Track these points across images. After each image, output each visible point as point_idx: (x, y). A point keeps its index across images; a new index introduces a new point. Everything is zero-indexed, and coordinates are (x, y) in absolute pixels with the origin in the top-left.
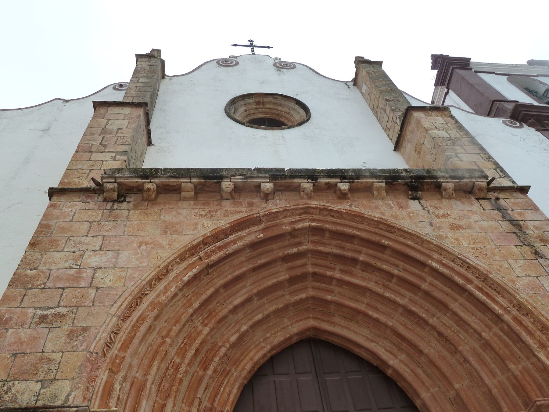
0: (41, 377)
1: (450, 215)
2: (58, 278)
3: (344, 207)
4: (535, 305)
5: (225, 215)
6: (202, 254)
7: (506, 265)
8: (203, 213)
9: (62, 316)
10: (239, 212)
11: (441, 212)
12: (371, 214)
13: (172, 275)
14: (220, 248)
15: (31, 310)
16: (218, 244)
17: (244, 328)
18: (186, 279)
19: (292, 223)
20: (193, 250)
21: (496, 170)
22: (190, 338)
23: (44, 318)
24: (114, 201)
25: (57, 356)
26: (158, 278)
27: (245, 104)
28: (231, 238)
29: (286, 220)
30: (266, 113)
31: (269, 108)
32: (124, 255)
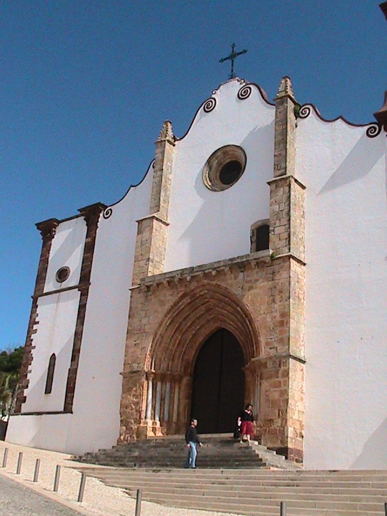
0: (138, 362)
1: (251, 281)
2: (137, 330)
3: (214, 283)
4: (259, 328)
5: (178, 294)
6: (171, 313)
7: (259, 309)
8: (172, 293)
9: (138, 343)
10: (182, 291)
11: (249, 279)
12: (223, 285)
13: (164, 323)
14: (178, 309)
15: (133, 342)
16: (176, 308)
17: (194, 332)
18: (168, 324)
19: (201, 291)
20: (168, 313)
21: (286, 239)
22: (175, 341)
23: (135, 344)
24: (147, 292)
25: (139, 356)
26: (160, 326)
27: (216, 159)
28: (180, 304)
29: (197, 291)
30: (231, 158)
31: (231, 154)
32: (151, 317)
